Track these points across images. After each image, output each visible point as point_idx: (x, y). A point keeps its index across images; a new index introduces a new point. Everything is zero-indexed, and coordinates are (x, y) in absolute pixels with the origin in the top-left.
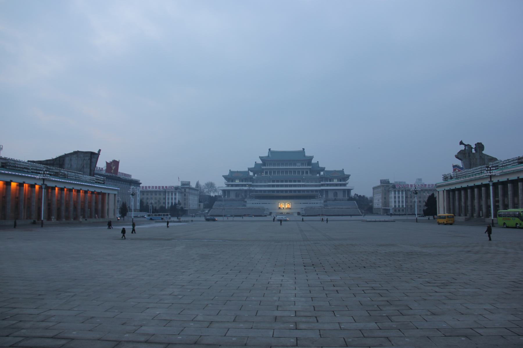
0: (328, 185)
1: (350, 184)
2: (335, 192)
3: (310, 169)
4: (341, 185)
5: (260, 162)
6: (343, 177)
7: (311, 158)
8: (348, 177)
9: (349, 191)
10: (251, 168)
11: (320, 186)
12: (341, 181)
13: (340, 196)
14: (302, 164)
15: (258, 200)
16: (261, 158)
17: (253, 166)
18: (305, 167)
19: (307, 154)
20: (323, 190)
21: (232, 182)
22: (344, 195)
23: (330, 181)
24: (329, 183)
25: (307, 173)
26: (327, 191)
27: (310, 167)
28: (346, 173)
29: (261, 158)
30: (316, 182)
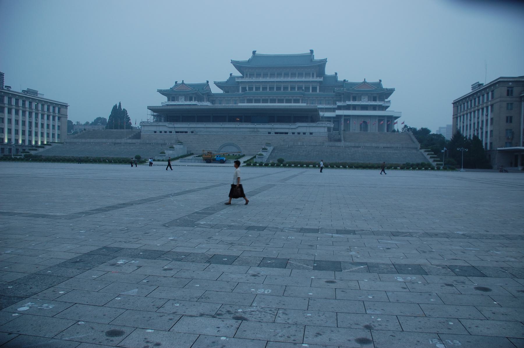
0: (348, 107)
1: (395, 105)
2: (364, 122)
3: (320, 82)
4: (374, 108)
5: (237, 73)
6: (380, 94)
7: (322, 64)
8: (389, 92)
9: (391, 119)
10: (220, 83)
11: (334, 110)
12: (375, 100)
13: (373, 127)
14: (308, 75)
15: (167, 124)
16: (238, 65)
17: (224, 78)
18: (311, 79)
19: (317, 57)
20: (339, 117)
21: (173, 100)
22: (380, 128)
23: (354, 99)
24: (351, 103)
25: (314, 89)
26: (347, 118)
27: (321, 79)
28: (386, 85)
29: (238, 65)
30: (329, 104)
